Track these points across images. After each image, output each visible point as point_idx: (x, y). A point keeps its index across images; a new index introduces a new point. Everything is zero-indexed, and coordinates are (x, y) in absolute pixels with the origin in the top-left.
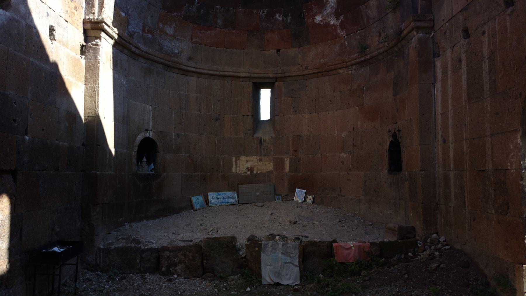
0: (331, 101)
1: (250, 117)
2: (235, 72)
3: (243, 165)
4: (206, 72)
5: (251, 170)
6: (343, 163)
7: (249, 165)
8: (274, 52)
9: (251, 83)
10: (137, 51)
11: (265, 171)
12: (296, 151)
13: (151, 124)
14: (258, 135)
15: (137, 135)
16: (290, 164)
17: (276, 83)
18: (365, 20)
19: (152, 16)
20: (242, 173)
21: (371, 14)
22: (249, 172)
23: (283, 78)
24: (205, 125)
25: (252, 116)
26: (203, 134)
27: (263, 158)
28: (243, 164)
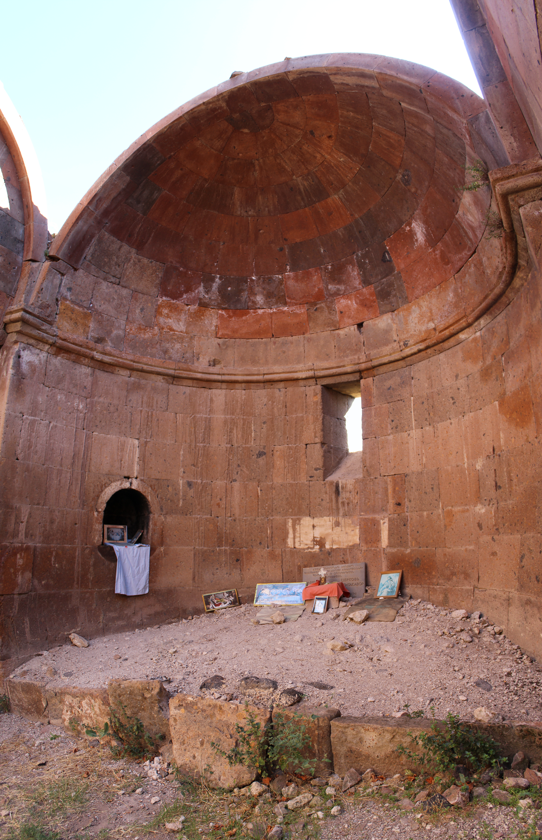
0: (453, 398)
1: (319, 446)
2: (288, 372)
3: (306, 533)
5: (321, 543)
7: (318, 533)
8: (352, 328)
9: (319, 387)
10: (107, 359)
11: (344, 546)
12: (399, 504)
13: (136, 468)
15: (106, 485)
16: (389, 531)
17: (362, 381)
19: (142, 310)
20: (304, 549)
22: (318, 547)
23: (371, 370)
24: (239, 466)
25: (323, 444)
26: (235, 480)
27: (341, 520)
28: (306, 533)
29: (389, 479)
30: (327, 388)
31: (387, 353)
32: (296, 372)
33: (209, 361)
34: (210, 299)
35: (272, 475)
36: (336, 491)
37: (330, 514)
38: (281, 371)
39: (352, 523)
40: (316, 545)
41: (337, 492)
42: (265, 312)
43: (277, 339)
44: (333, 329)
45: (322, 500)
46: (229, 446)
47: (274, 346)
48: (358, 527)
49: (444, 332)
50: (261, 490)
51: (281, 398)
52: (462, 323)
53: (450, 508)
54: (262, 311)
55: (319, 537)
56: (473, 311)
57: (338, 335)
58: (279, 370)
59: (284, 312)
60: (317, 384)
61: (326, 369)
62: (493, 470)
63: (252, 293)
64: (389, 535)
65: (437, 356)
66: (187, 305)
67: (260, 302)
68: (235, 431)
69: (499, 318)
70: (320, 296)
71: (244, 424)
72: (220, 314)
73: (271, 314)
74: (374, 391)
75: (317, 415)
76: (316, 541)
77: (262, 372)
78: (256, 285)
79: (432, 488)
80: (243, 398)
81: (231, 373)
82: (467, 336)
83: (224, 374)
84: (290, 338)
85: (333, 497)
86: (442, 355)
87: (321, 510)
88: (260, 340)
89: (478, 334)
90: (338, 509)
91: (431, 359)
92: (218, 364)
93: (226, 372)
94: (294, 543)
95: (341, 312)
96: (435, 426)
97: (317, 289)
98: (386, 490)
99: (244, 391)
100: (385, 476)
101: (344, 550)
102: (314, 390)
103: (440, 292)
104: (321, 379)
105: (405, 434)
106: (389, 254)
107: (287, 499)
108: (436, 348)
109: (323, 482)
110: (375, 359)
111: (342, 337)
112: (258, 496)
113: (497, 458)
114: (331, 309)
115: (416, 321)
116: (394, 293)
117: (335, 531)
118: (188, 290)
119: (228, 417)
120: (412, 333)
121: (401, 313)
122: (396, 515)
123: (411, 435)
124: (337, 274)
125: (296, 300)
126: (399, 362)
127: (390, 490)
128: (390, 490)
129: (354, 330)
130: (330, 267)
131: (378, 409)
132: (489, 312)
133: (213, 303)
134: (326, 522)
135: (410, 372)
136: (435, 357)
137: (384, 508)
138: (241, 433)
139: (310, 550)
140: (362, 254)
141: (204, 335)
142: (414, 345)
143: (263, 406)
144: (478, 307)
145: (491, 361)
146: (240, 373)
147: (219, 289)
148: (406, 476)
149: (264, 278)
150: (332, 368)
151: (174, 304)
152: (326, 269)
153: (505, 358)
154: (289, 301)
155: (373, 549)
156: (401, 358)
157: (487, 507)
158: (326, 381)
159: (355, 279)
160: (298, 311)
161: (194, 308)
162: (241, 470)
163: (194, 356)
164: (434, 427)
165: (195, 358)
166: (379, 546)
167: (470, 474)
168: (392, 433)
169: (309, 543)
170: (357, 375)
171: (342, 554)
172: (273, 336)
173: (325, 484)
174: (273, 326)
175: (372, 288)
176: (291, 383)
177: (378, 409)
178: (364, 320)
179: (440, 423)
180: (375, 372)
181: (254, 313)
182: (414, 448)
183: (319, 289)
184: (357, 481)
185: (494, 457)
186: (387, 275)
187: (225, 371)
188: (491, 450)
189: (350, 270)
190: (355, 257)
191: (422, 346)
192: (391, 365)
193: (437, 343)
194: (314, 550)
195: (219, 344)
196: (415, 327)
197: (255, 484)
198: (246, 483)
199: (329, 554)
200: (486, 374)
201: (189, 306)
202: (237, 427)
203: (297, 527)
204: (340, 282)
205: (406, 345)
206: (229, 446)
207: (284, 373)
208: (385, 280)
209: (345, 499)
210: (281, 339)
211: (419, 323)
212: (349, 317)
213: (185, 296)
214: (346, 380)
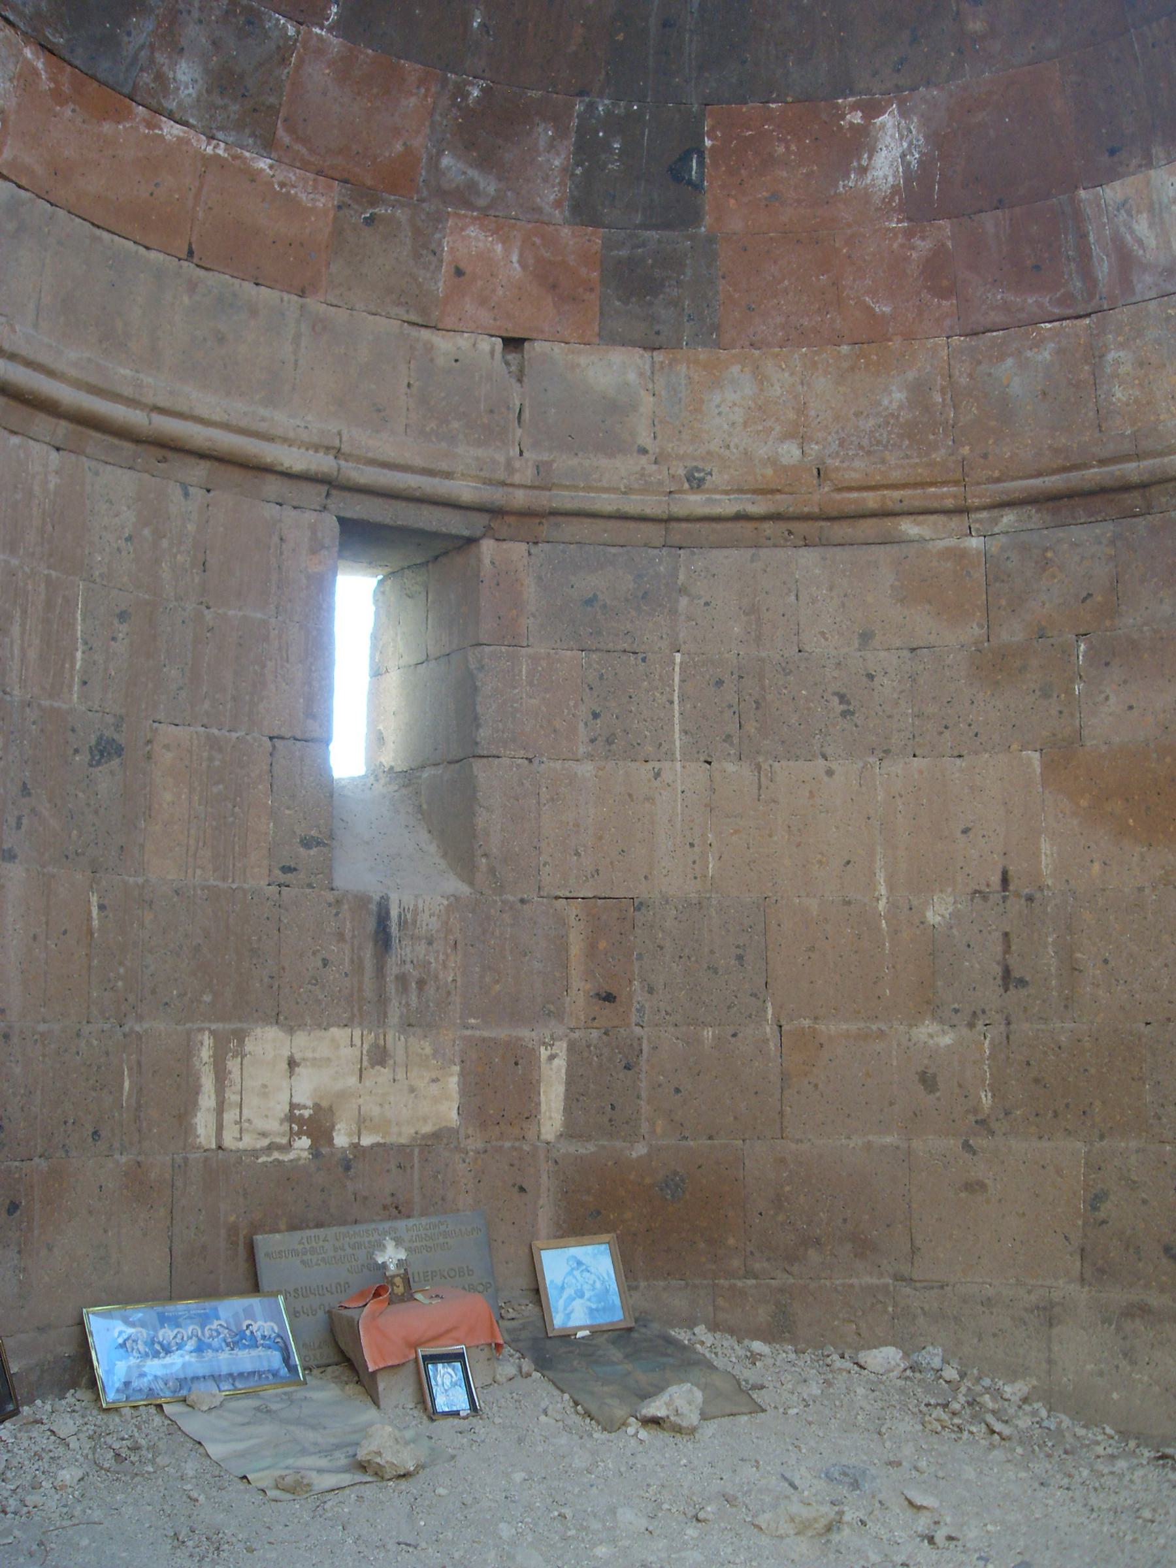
0: (842, 698)
3: (264, 1092)
6: (928, 1081)
7: (305, 1090)
11: (402, 1135)
12: (609, 998)
14: (356, 873)
16: (570, 1082)
17: (487, 547)
18: (1103, 269)
20: (255, 1153)
21: (1151, 242)
22: (305, 1142)
24: (25, 790)
27: (396, 1042)
29: (573, 910)
31: (614, 480)
32: (269, 438)
35: (142, 846)
36: (377, 932)
37: (352, 1018)
38: (216, 417)
39: (436, 1052)
40: (300, 1134)
41: (383, 939)
42: (188, 142)
43: (202, 273)
44: (413, 318)
45: (325, 962)
47: (186, 299)
48: (457, 1069)
49: (855, 495)
50: (102, 907)
51: (191, 527)
52: (943, 497)
53: (807, 1023)
55: (310, 1103)
56: (998, 480)
57: (429, 348)
58: (209, 411)
59: (253, 176)
60: (325, 508)
62: (998, 935)
64: (566, 1098)
67: (183, 93)
69: (1077, 533)
70: (399, 179)
71: (49, 605)
74: (530, 591)
76: (301, 1121)
77: (149, 399)
78: (196, 14)
79: (740, 958)
80: (52, 486)
84: (248, 286)
85: (368, 954)
86: (808, 558)
87: (319, 1002)
88: (142, 250)
89: (975, 543)
90: (382, 1001)
91: (764, 552)
93: (26, 351)
94: (220, 1128)
95: (459, 272)
96: (765, 766)
97: (399, 147)
98: (561, 946)
99: (54, 455)
100: (557, 898)
101: (402, 1150)
102: (313, 528)
103: (852, 369)
104: (347, 494)
105: (645, 771)
106: (701, 164)
107: (197, 949)
108: (795, 526)
110: (567, 487)
111: (440, 361)
112: (90, 933)
113: (1016, 906)
114: (425, 246)
115: (738, 416)
116: (675, 293)
117: (368, 1083)
120: (714, 447)
121: (682, 369)
122: (595, 1034)
123: (667, 776)
124: (487, 131)
126: (643, 526)
127: (576, 948)
128: (576, 948)
129: (492, 353)
131: (544, 663)
132: (1051, 504)
134: (338, 1047)
135: (676, 569)
136: (782, 554)
137: (552, 1007)
138: (37, 642)
139: (276, 1155)
140: (609, 113)
142: (727, 493)
144: (1021, 478)
145: (1019, 637)
146: (73, 372)
148: (638, 909)
152: (460, 91)
153: (1091, 647)
155: (507, 1144)
156: (665, 516)
157: (965, 1031)
158: (361, 508)
159: (546, 179)
160: (303, 197)
162: (33, 810)
164: (759, 767)
166: (531, 1135)
167: (896, 932)
168: (590, 757)
169: (274, 1126)
170: (482, 520)
171: (394, 1167)
173: (338, 902)
174: (201, 215)
175: (596, 239)
176: (236, 474)
177: (544, 663)
178: (534, 336)
179: (784, 763)
181: (150, 125)
182: (668, 819)
183: (408, 149)
184: (455, 902)
185: (1005, 899)
186: (668, 226)
188: (996, 879)
189: (542, 144)
190: (579, 107)
192: (611, 524)
194: (292, 1156)
196: (730, 434)
197: (79, 876)
198: (51, 869)
199: (348, 1168)
200: (995, 665)
202: (24, 612)
203: (233, 1065)
204: (487, 162)
207: (226, 426)
208: (654, 235)
209: (409, 967)
211: (745, 424)
212: (483, 301)
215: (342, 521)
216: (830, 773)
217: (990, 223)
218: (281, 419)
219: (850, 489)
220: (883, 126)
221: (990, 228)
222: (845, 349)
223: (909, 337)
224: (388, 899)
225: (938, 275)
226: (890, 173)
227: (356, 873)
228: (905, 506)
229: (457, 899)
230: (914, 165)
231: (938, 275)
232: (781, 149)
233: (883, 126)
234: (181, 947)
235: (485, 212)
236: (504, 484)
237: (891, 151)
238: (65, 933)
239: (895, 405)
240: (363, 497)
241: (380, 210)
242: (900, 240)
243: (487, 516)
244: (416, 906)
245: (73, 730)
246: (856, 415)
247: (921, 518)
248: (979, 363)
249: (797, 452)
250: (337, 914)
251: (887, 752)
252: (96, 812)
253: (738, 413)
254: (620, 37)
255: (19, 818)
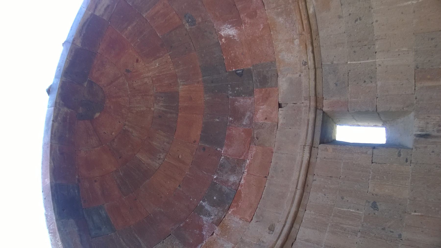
0: (356, 21)
1: (375, 151)
4: (294, 209)
8: (280, 112)
9: (322, 146)
14: (408, 141)
17: (325, 109)
23: (318, 100)
26: (400, 235)
29: (419, 85)
30: (322, 142)
31: (307, 82)
32: (302, 161)
33: (269, 233)
34: (216, 215)
35: (399, 199)
36: (425, 138)
41: (426, 136)
42: (245, 178)
45: (433, 152)
46: (359, 234)
47: (275, 178)
49: (304, 26)
50: (415, 212)
52: (302, 5)
54: (242, 180)
57: (282, 124)
58: (297, 175)
59: (250, 164)
60: (317, 148)
61: (307, 135)
63: (226, 182)
65: (320, 38)
66: (212, 234)
68: (345, 226)
70: (249, 133)
72: (231, 213)
73: (248, 174)
75: (346, 150)
77: (294, 189)
78: (221, 177)
79: (432, 39)
80: (313, 213)
81: (286, 215)
82: (312, 6)
83: (286, 222)
84: (272, 164)
85: (431, 140)
86: (321, 34)
91: (321, 45)
92: (274, 228)
95: (266, 119)
96: (376, 38)
97: (243, 133)
99: (307, 211)
100: (415, 89)
103: (276, 31)
106: (238, 70)
108: (314, 38)
109: (414, 150)
112: (422, 216)
116: (265, 72)
118: (201, 228)
119: (328, 228)
121: (281, 68)
124: (238, 115)
125: (245, 152)
126: (317, 74)
128: (430, 84)
129: (282, 110)
130: (231, 119)
133: (220, 214)
140: (231, 91)
141: (244, 231)
142: (307, 56)
143: (326, 197)
146: (289, 208)
147: (211, 206)
148: (418, 68)
149: (219, 170)
150: (307, 130)
151: (206, 244)
152: (231, 122)
154: (243, 157)
159: (246, 102)
161: (217, 230)
162: (389, 227)
163: (260, 245)
165: (262, 244)
168: (376, 82)
170: (318, 111)
172: (266, 177)
173: (416, 148)
175: (256, 90)
176: (311, 168)
180: (320, 96)
187: (283, 220)
189: (239, 104)
191: (310, 48)
192: (317, 81)
193: (311, 35)
195: (257, 222)
198: (404, 224)
201: (214, 234)
202: (341, 224)
204: (244, 115)
205: (305, 64)
206: (359, 234)
207: (300, 172)
210: (271, 172)
212: (271, 113)
213: (204, 233)
214: (321, 122)
215: (320, 144)
216: (377, 21)
217: (239, 6)
218: (298, 158)
219: (303, 27)
220: (224, 34)
221: (240, 6)
222: (272, 33)
223: (267, 19)
224: (415, 135)
225: (253, 15)
226: (233, 30)
227: (408, 141)
228: (306, 14)
229: (415, 116)
230: (231, 26)
231: (253, 15)
232: (233, 54)
233: (224, 34)
234: (427, 191)
235: (254, 114)
236: (310, 107)
237: (228, 31)
238: (422, 223)
239: (283, 20)
240: (314, 139)
241: (255, 136)
242: (246, 25)
243: (317, 110)
244: (417, 127)
245: (369, 214)
246: (286, 28)
247: (308, 9)
248: (270, 2)
249: (297, 40)
250: (419, 148)
251: (370, 7)
252: (390, 210)
253: (289, 55)
254: (216, 91)
255: (391, 232)
